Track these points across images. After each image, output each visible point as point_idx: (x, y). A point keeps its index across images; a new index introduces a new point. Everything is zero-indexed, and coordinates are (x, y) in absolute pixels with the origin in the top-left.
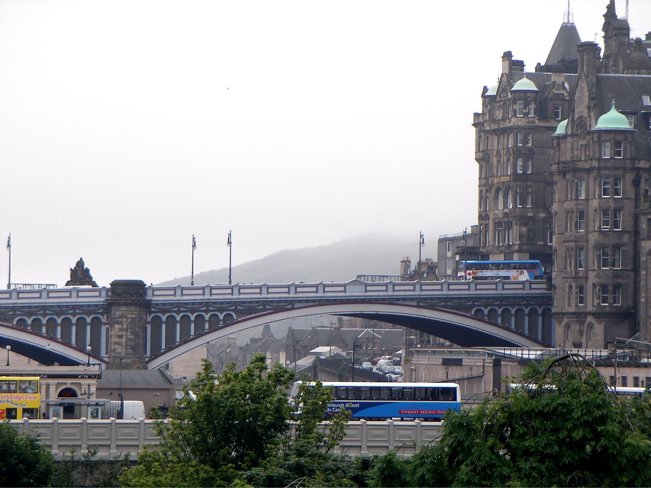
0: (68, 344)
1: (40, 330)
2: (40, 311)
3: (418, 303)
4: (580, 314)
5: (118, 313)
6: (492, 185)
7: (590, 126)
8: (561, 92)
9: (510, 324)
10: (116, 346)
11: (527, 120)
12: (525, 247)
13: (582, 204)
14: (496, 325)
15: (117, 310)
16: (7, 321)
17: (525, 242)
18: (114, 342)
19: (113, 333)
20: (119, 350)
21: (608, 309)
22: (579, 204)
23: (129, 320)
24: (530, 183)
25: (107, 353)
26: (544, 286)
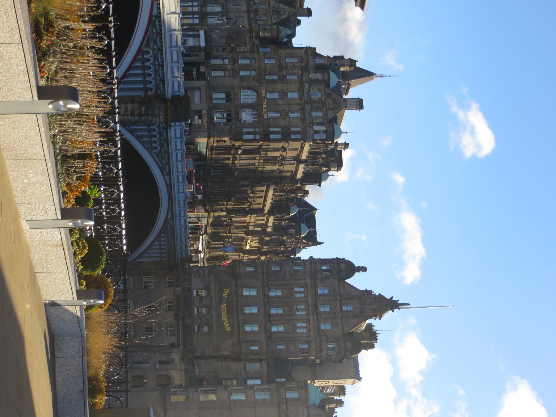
18: (127, 107)
26: (184, 255)
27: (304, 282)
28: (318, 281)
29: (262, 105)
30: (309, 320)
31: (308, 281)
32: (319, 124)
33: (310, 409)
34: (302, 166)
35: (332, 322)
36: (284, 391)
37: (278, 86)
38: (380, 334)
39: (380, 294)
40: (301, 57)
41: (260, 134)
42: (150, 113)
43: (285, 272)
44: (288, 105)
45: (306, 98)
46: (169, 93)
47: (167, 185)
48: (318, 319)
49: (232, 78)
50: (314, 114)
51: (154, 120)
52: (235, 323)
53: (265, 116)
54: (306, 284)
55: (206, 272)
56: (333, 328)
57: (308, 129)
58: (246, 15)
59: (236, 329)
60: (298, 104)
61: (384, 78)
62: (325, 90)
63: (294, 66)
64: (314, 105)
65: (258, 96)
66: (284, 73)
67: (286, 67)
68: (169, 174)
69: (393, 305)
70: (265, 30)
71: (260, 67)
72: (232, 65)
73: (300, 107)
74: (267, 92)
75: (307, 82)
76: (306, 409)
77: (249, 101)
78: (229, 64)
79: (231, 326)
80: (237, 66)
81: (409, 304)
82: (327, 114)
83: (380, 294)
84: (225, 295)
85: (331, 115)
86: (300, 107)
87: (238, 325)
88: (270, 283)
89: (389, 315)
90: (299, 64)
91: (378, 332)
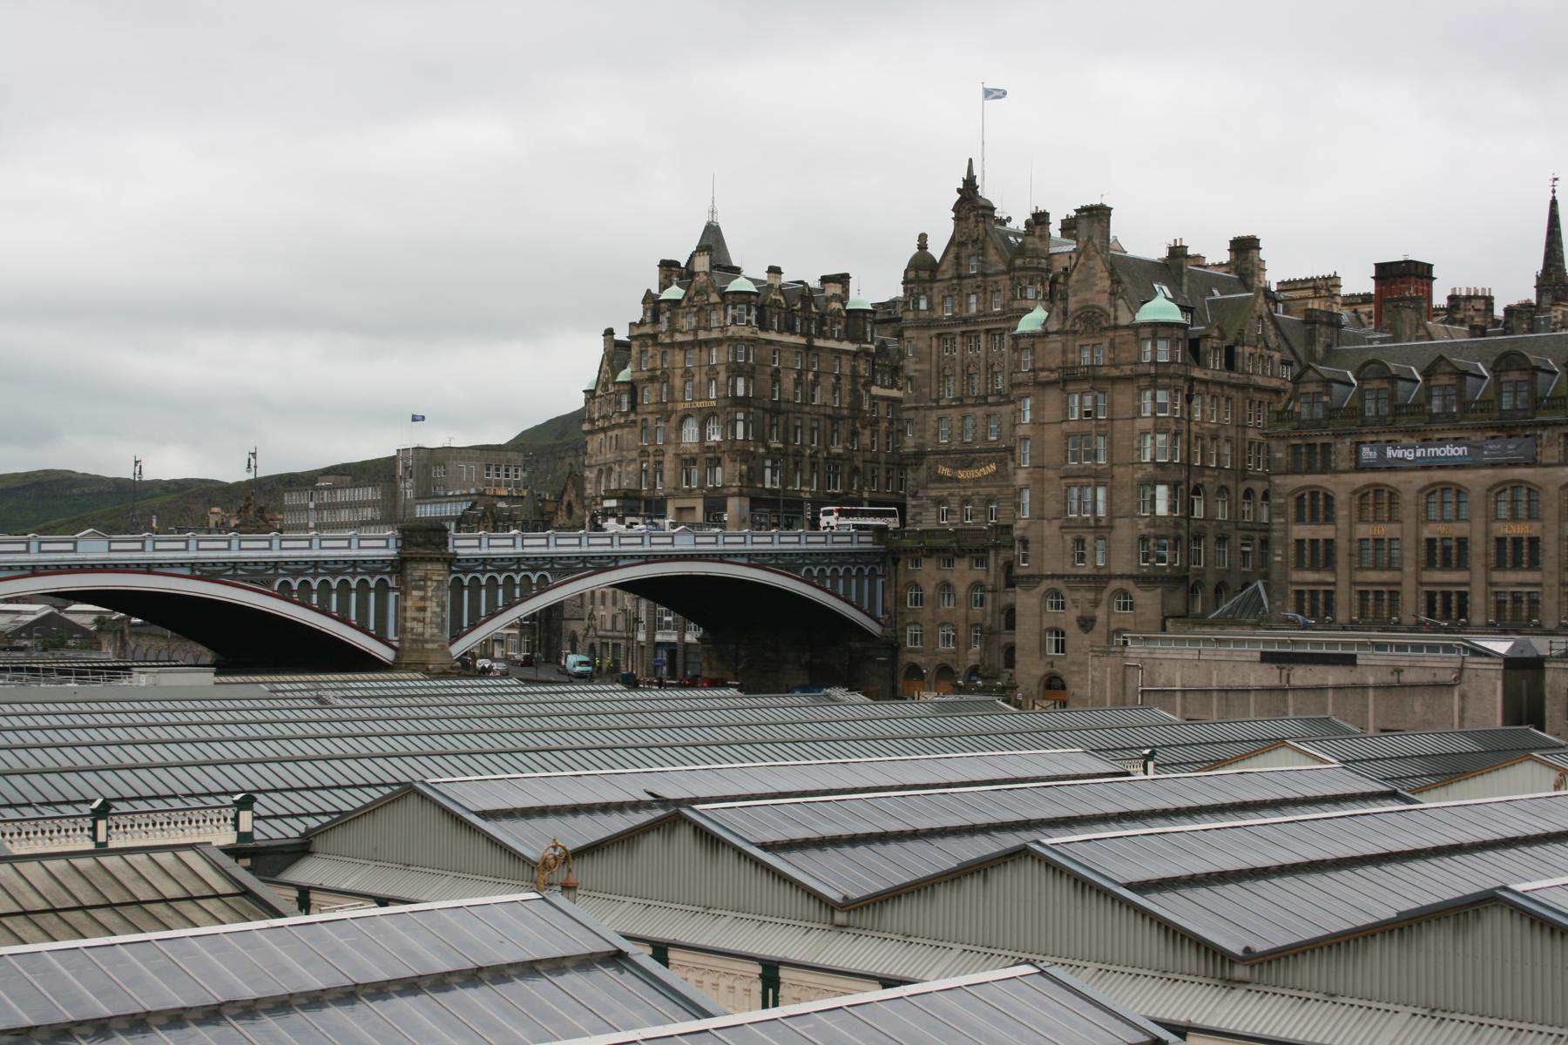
0: (345, 620)
1: (310, 599)
2: (309, 569)
3: (749, 560)
4: (1101, 577)
5: (418, 574)
6: (674, 412)
7: (1116, 318)
8: (778, 298)
9: (837, 586)
10: (414, 624)
11: (750, 330)
12: (745, 490)
13: (1104, 426)
14: (824, 590)
15: (416, 569)
16: (263, 583)
17: (745, 484)
19: (409, 603)
20: (420, 630)
21: (1168, 570)
22: (1100, 426)
23: (435, 584)
24: (752, 410)
25: (396, 635)
26: (870, 539)
27: (934, 341)
28: (935, 316)
29: (700, 409)
30: (988, 331)
31: (934, 332)
32: (725, 318)
33: (1050, 330)
34: (819, 343)
35: (993, 292)
36: (1019, 375)
37: (678, 382)
38: (1037, 208)
39: (953, 210)
40: (641, 346)
41: (736, 413)
42: (422, 583)
43: (916, 371)
44: (700, 366)
45: (689, 338)
46: (391, 553)
47: (647, 562)
48: (985, 316)
49: (666, 457)
50: (714, 324)
51: (435, 578)
52: (985, 455)
53: (714, 403)
54: (939, 336)
55: (914, 503)
56: (999, 291)
57: (729, 334)
58: (609, 434)
59: (994, 454)
60: (700, 351)
61: (718, 207)
62: (684, 308)
63: (652, 357)
64: (702, 325)
65: (690, 416)
66: (659, 372)
67: (653, 370)
68: (616, 559)
69: (969, 188)
70: (619, 403)
71: (652, 413)
72: (649, 456)
73: (704, 348)
74: (684, 401)
75: (673, 336)
76: (1052, 337)
77: (696, 429)
78: (648, 461)
79: (990, 462)
80: (651, 449)
81: (971, 160)
82: (714, 304)
83: (953, 210)
84: (946, 471)
85: (714, 298)
86: (704, 348)
87: (986, 451)
88: (934, 397)
89: (987, 191)
90: (650, 349)
91: (1034, 211)
